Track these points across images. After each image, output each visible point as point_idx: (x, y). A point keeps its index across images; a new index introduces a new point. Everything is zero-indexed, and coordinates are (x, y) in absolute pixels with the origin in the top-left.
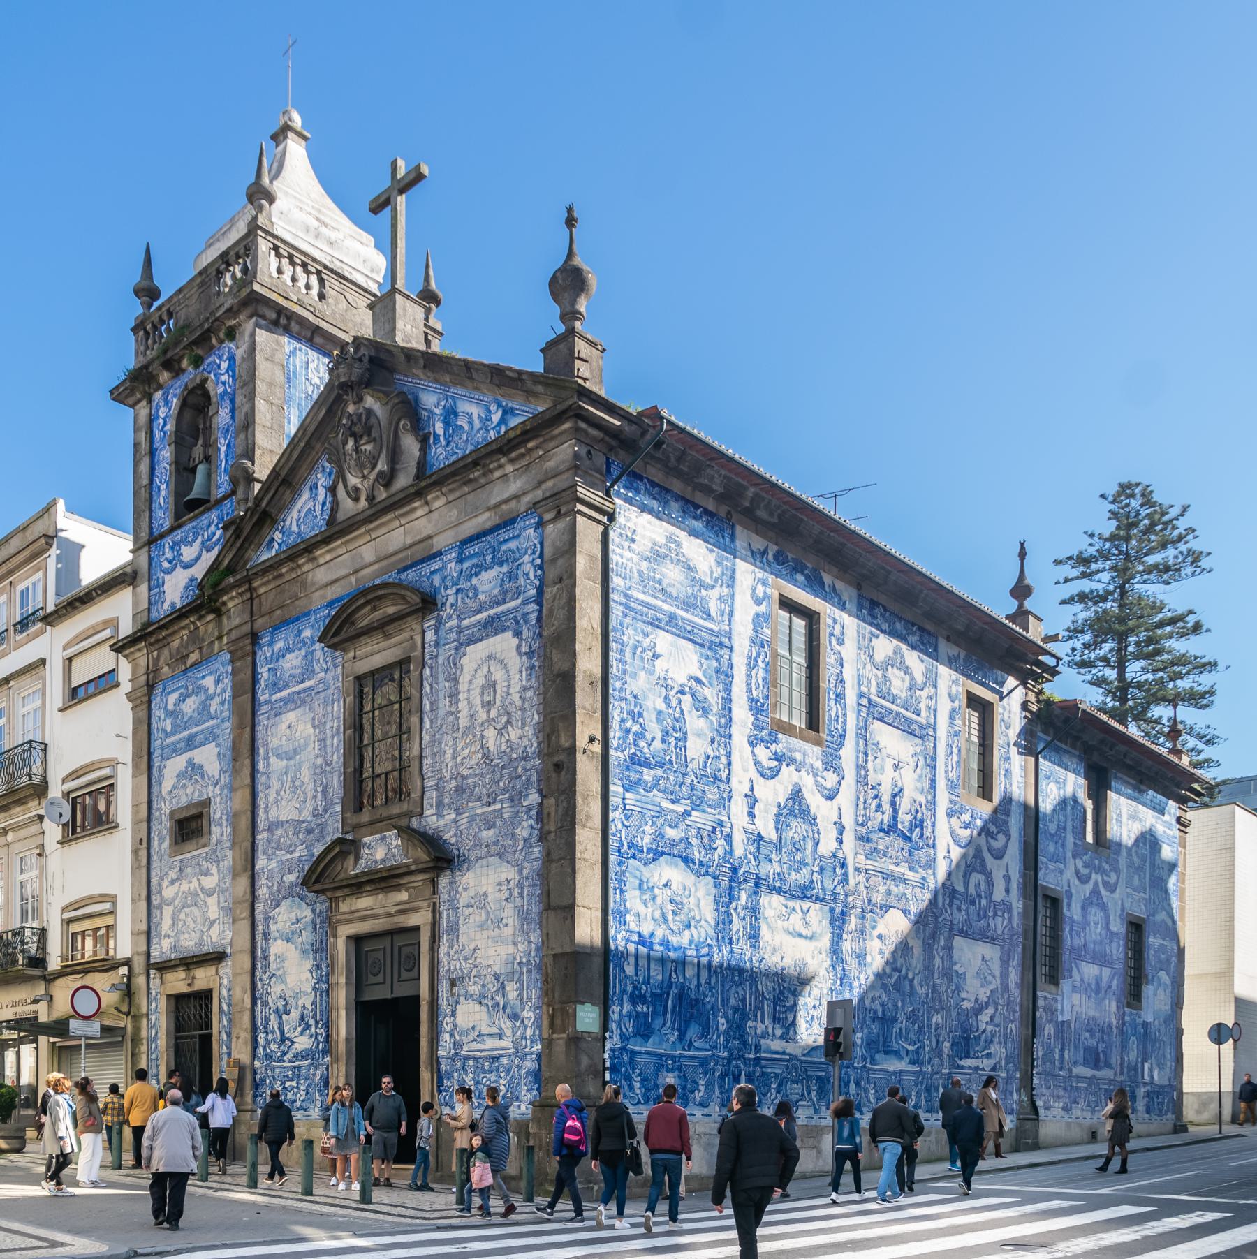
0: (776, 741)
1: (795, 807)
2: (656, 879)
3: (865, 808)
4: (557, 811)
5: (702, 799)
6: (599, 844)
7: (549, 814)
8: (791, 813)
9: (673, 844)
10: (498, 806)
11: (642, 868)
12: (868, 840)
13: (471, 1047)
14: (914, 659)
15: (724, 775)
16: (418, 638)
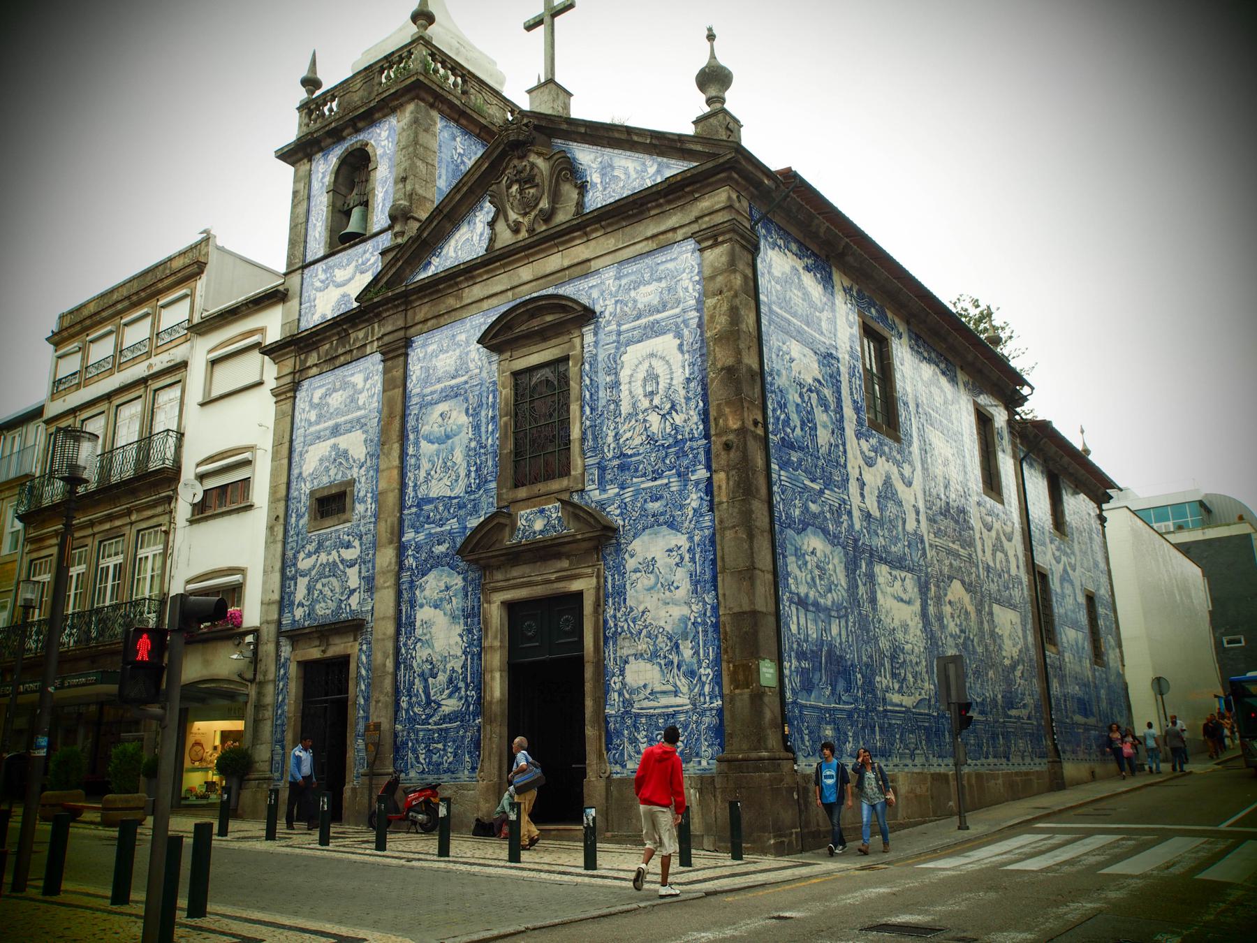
0: (871, 436)
1: (887, 494)
2: (805, 547)
4: (728, 483)
5: (830, 479)
6: (766, 514)
7: (720, 487)
9: (815, 516)
10: (666, 481)
12: (935, 522)
13: (641, 704)
14: (943, 381)
15: (842, 461)
16: (577, 341)
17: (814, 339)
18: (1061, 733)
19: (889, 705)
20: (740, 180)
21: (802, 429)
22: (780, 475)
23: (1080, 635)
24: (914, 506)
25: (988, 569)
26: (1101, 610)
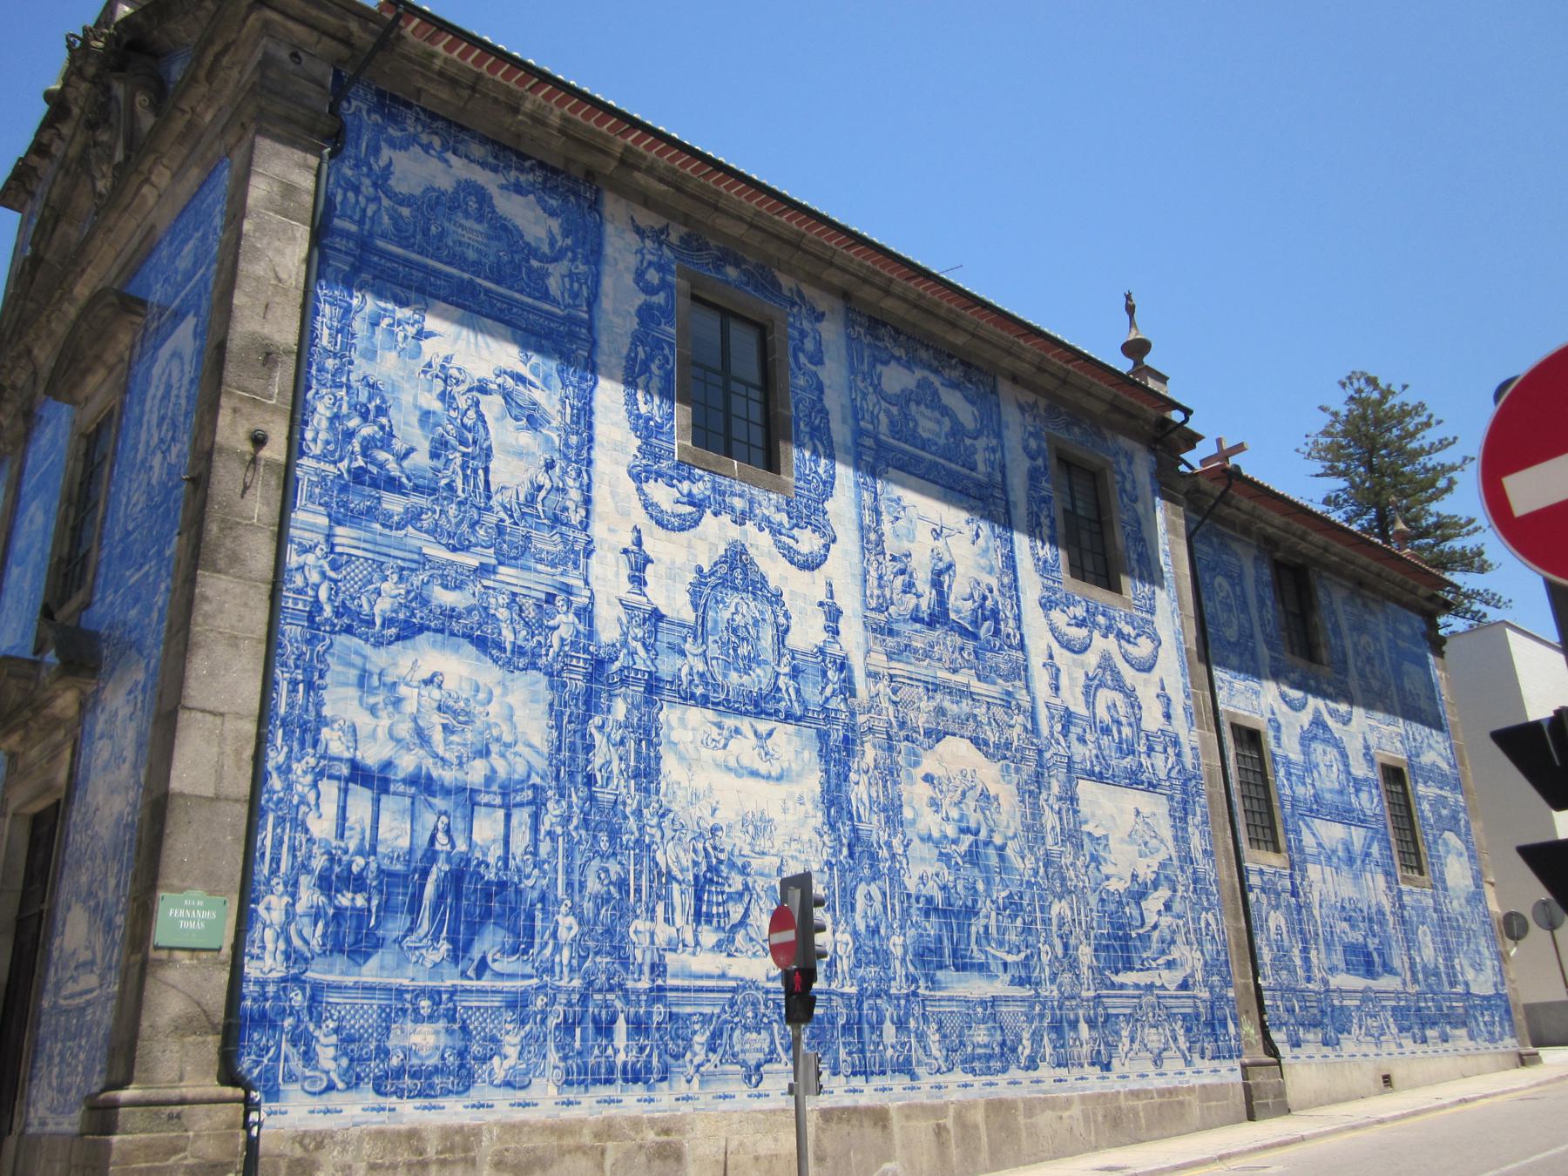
0: (691, 478)
3: (880, 586)
5: (526, 549)
8: (726, 583)
9: (451, 614)
11: (368, 649)
12: (891, 632)
15: (576, 518)
17: (512, 303)
18: (1291, 1011)
19: (675, 976)
20: (291, 25)
21: (434, 455)
22: (329, 536)
23: (1358, 836)
24: (821, 604)
25: (1068, 718)
26: (1424, 792)
